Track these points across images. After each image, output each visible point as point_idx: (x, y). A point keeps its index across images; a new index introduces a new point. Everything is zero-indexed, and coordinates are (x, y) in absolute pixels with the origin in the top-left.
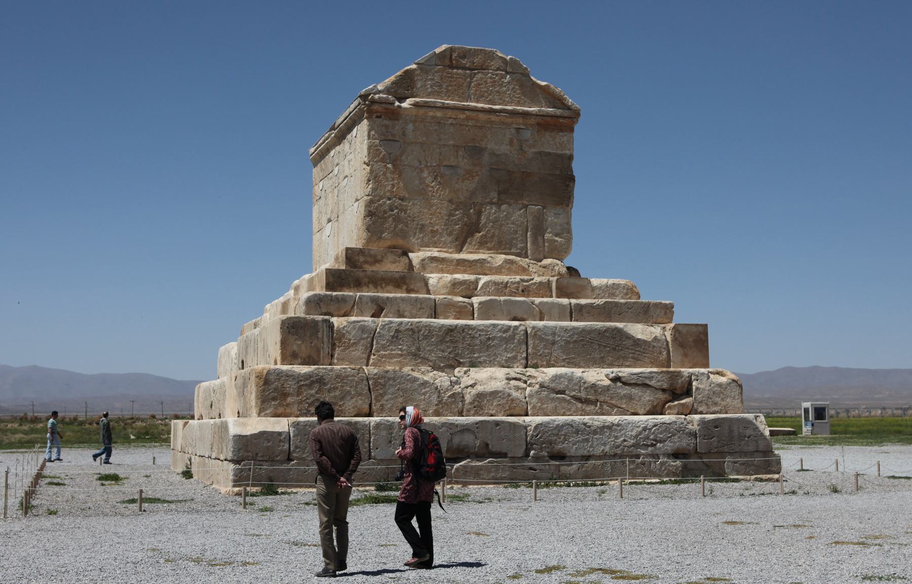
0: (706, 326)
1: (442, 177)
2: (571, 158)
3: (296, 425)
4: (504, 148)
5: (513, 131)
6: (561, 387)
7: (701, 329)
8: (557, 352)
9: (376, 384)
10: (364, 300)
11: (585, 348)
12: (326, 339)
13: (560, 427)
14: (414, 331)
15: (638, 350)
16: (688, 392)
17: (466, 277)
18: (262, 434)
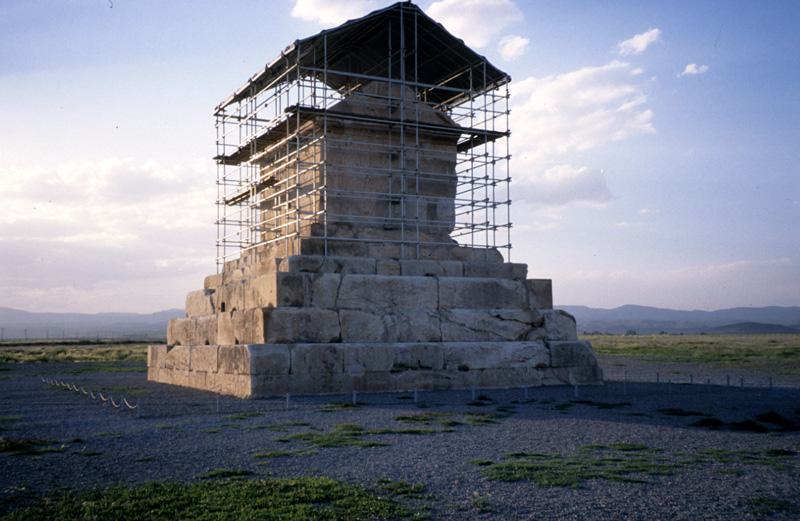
0: (550, 281)
6: (462, 322)
14: (365, 283)
16: (542, 324)
18: (275, 356)
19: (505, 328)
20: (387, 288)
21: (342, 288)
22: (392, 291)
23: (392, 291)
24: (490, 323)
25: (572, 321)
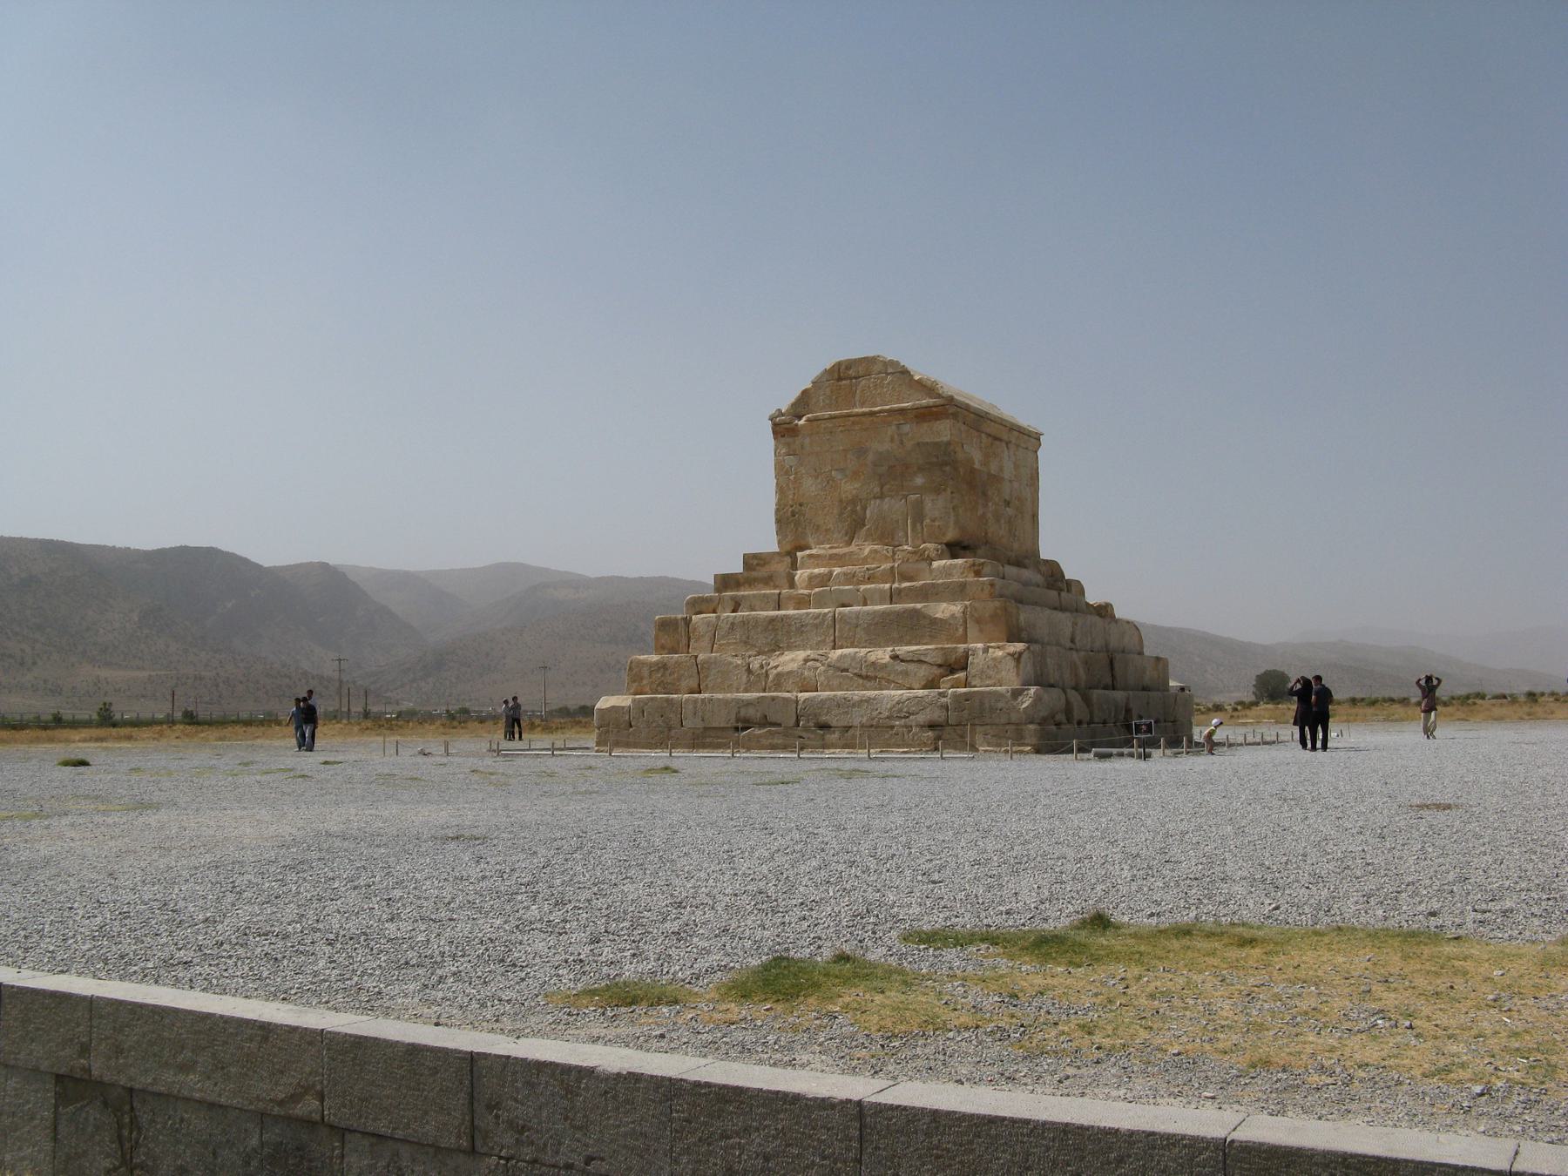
3: (634, 701)
4: (886, 446)
8: (860, 633)
11: (881, 629)
13: (823, 702)
14: (745, 623)
15: (935, 628)
16: (965, 668)
17: (822, 570)
19: (906, 673)
23: (775, 630)
24: (885, 666)
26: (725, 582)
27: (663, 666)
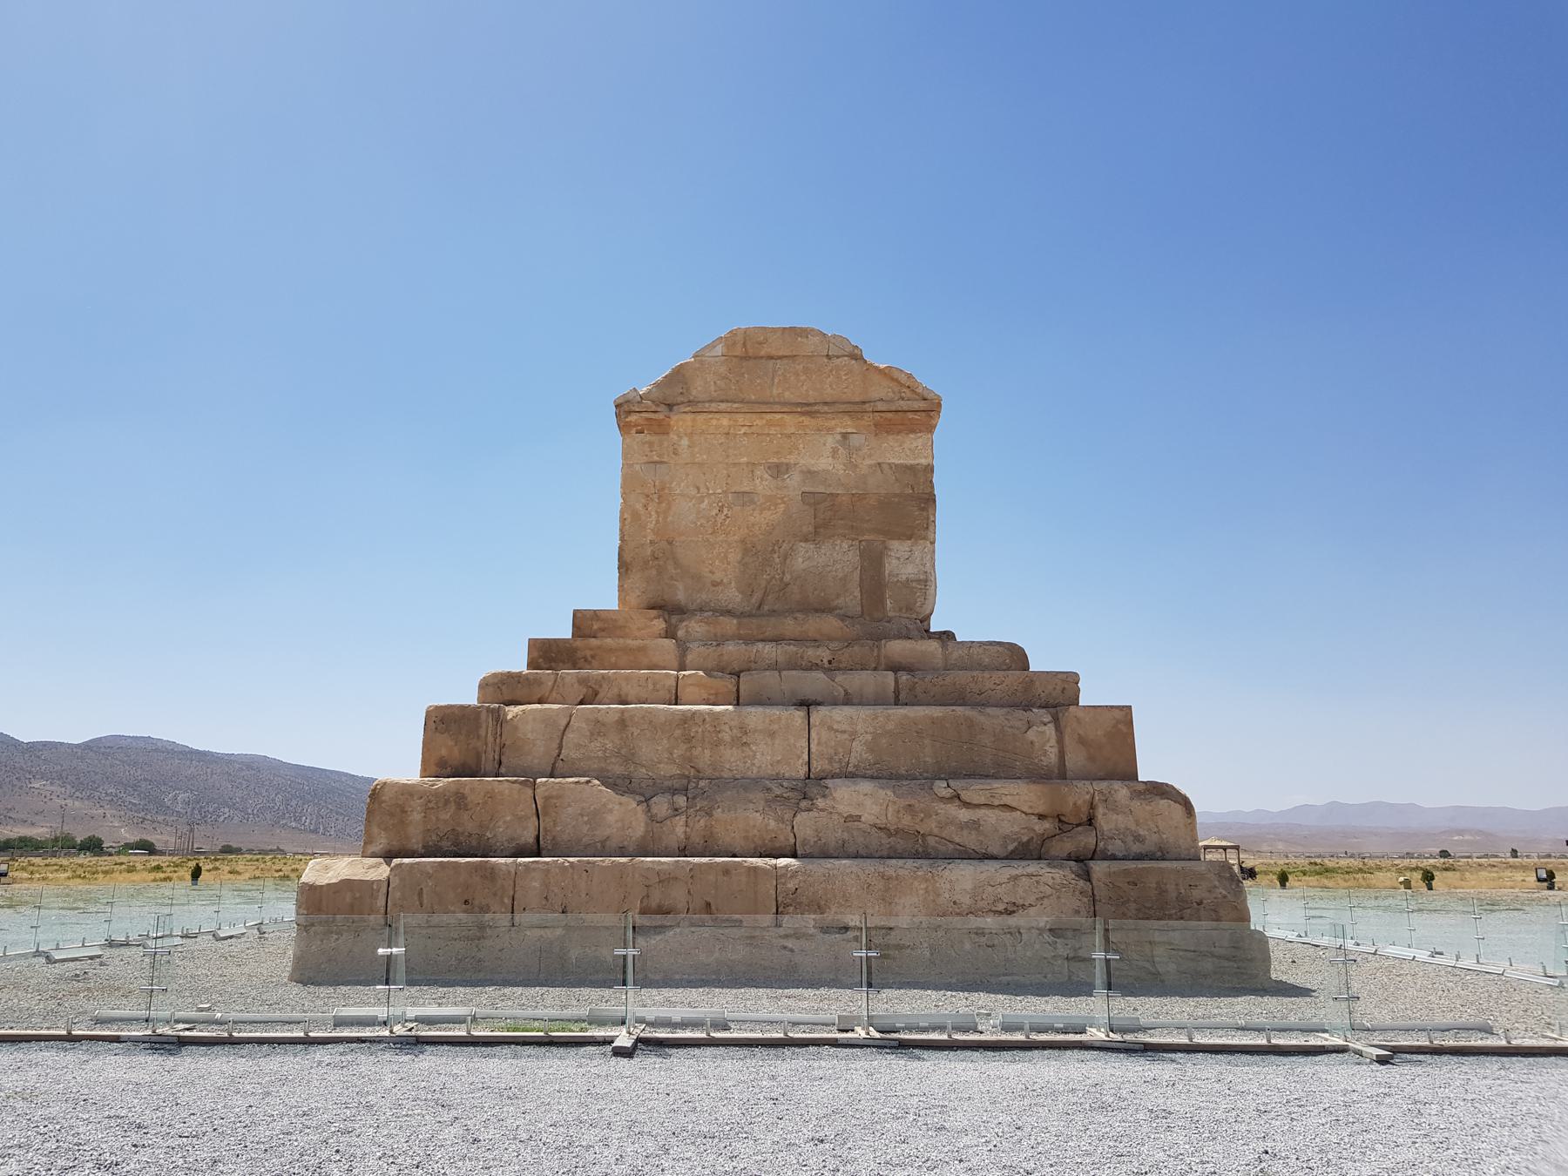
0: (1127, 710)
1: (730, 508)
2: (930, 469)
4: (824, 463)
5: (839, 437)
7: (1118, 714)
9: (544, 807)
10: (568, 679)
12: (490, 739)
14: (622, 723)
16: (1091, 821)
19: (975, 825)
20: (678, 732)
21: (570, 735)
22: (688, 739)
23: (688, 739)
25: (1178, 810)
26: (545, 653)
27: (460, 800)
